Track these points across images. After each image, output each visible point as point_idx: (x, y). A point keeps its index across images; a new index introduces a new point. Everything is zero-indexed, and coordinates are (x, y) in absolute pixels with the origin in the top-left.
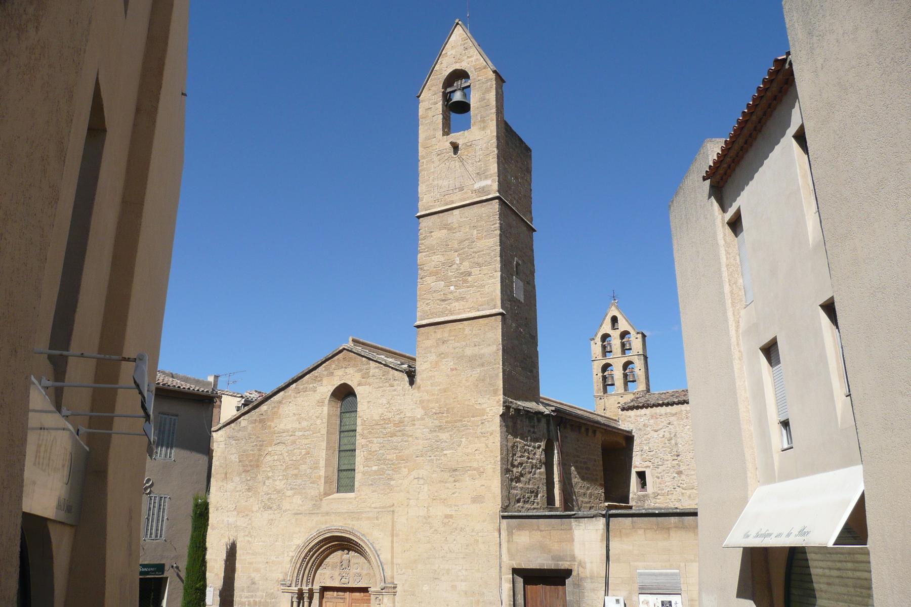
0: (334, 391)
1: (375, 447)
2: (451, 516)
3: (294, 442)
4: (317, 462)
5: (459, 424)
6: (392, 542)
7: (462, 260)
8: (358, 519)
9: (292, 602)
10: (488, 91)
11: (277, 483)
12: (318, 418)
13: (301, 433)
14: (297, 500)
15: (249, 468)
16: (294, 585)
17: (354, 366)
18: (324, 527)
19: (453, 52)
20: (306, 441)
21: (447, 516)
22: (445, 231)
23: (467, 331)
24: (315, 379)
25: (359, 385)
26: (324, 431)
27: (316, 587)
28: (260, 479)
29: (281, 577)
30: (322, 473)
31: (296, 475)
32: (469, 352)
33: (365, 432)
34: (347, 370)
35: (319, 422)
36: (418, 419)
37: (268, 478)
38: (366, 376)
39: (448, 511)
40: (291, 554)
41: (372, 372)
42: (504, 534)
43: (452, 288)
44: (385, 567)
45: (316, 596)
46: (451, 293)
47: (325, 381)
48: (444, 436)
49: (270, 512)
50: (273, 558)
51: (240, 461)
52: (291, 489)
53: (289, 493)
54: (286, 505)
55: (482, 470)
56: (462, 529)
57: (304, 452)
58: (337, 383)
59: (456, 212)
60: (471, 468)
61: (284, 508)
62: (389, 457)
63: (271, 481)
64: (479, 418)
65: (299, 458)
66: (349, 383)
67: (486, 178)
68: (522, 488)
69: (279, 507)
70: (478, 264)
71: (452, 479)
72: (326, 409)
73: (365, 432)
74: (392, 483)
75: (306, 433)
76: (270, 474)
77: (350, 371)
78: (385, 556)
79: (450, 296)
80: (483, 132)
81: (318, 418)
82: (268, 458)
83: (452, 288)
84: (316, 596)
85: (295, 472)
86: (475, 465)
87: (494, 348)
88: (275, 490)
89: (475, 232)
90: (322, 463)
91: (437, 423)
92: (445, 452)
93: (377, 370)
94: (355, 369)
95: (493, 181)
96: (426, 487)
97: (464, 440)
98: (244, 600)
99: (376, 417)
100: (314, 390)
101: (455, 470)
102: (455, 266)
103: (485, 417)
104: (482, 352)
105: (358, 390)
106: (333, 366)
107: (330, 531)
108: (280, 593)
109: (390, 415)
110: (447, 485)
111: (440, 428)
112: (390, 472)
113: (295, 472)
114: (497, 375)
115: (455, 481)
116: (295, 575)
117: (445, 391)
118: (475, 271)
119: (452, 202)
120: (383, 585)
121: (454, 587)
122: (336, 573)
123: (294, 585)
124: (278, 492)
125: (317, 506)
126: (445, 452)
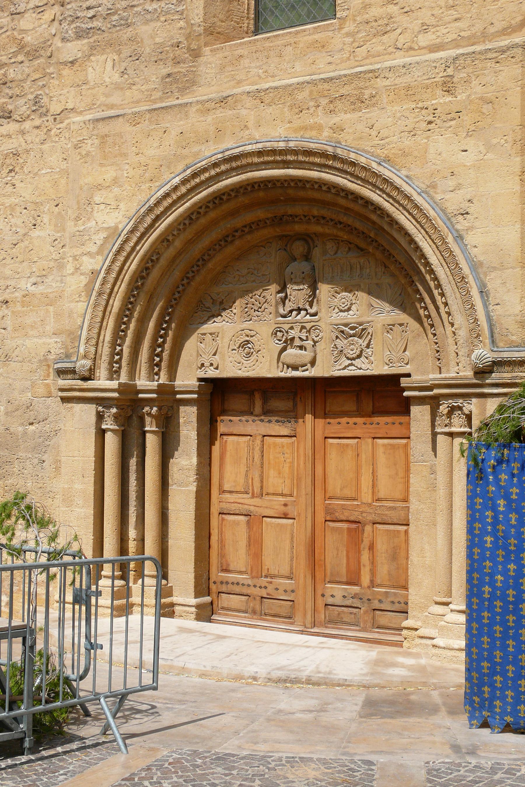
8: (359, 102)
9: (101, 433)
11: (27, 22)
14: (103, 70)
16: (102, 372)
18: (210, 152)
27: (187, 379)
29: (54, 346)
40: (90, 264)
44: (493, 282)
45: (188, 419)
50: (26, 285)
52: (80, 35)
53: (73, 49)
54: (61, 95)
61: (55, 108)
69: (38, 106)
78: (487, 236)
84: (188, 419)
107: (234, 162)
108: (54, 403)
116: (108, 335)
120: (484, 353)
123: (102, 372)
124: (33, 54)
125: (179, 82)
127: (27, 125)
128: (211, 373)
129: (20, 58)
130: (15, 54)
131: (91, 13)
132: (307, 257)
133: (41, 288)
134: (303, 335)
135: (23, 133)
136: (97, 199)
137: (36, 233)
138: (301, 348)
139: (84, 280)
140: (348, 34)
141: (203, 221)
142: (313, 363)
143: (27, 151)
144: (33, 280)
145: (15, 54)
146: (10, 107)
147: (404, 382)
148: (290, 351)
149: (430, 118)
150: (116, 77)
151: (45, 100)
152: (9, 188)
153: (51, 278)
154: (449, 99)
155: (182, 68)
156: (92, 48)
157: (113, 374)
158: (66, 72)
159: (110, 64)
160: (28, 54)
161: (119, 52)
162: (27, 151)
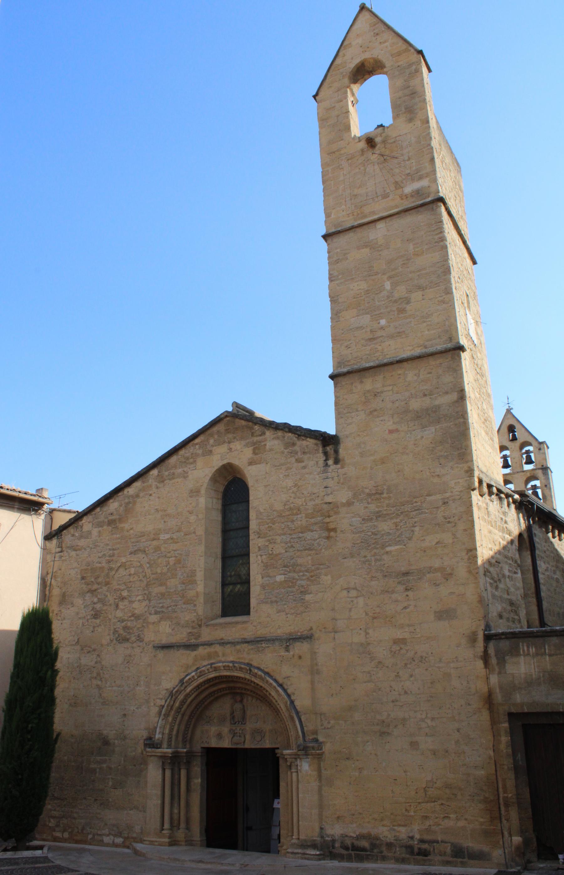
0: (214, 475)
1: (279, 549)
2: (403, 641)
3: (157, 548)
4: (193, 573)
5: (407, 508)
6: (312, 682)
7: (394, 285)
12: (191, 513)
13: (167, 536)
15: (95, 587)
16: (165, 745)
17: (242, 438)
19: (360, 41)
20: (175, 546)
21: (396, 642)
22: (366, 251)
24: (186, 462)
25: (250, 463)
26: (201, 531)
27: (197, 748)
28: (112, 601)
30: (200, 588)
31: (163, 595)
32: (415, 405)
33: (262, 528)
34: (232, 446)
35: (193, 518)
36: (344, 505)
37: (123, 599)
38: (257, 449)
39: (399, 634)
41: (269, 444)
43: (383, 322)
46: (382, 328)
47: (200, 462)
48: (385, 526)
49: (127, 645)
51: (83, 578)
52: (156, 613)
53: (153, 618)
55: (449, 570)
56: (422, 659)
57: (172, 560)
59: (381, 225)
60: (431, 570)
62: (300, 561)
63: (126, 602)
64: (439, 497)
65: (165, 570)
66: (236, 462)
67: (421, 178)
71: (401, 588)
72: (202, 501)
73: (262, 528)
74: (308, 597)
76: (125, 594)
77: (237, 445)
80: (411, 125)
81: (191, 513)
82: (122, 572)
85: (162, 589)
86: (437, 564)
88: (133, 615)
89: (411, 246)
90: (200, 576)
91: (373, 507)
92: (388, 549)
93: (276, 442)
94: (243, 443)
96: (361, 601)
97: (417, 529)
98: (93, 766)
99: (279, 507)
100: (185, 476)
101: (406, 574)
102: (385, 293)
103: (448, 495)
104: (437, 403)
106: (212, 441)
109: (299, 502)
110: (394, 596)
111: (379, 515)
112: (303, 583)
113: (162, 589)
115: (407, 590)
117: (383, 461)
118: (416, 296)
121: (414, 745)
122: (225, 730)
123: (165, 745)
126: (388, 549)
127: (135, 645)
128: (206, 745)
129: (132, 618)
130: (130, 617)
131: (161, 605)
132: (241, 701)
133: (140, 710)
134: (241, 732)
135: (133, 648)
136: (163, 677)
137: (138, 688)
138: (240, 736)
139: (157, 709)
140: (254, 626)
141: (203, 688)
142: (244, 742)
143: (135, 655)
144: (136, 706)
145: (130, 617)
146: (128, 637)
147: (277, 751)
148: (235, 738)
149: (281, 659)
150: (170, 631)
151: (142, 636)
152: (127, 669)
153: (144, 706)
154: (287, 653)
155: (195, 631)
156: (161, 619)
157: (169, 746)
158: (151, 626)
159: (168, 624)
160: (136, 617)
161: (172, 622)
162: (135, 655)
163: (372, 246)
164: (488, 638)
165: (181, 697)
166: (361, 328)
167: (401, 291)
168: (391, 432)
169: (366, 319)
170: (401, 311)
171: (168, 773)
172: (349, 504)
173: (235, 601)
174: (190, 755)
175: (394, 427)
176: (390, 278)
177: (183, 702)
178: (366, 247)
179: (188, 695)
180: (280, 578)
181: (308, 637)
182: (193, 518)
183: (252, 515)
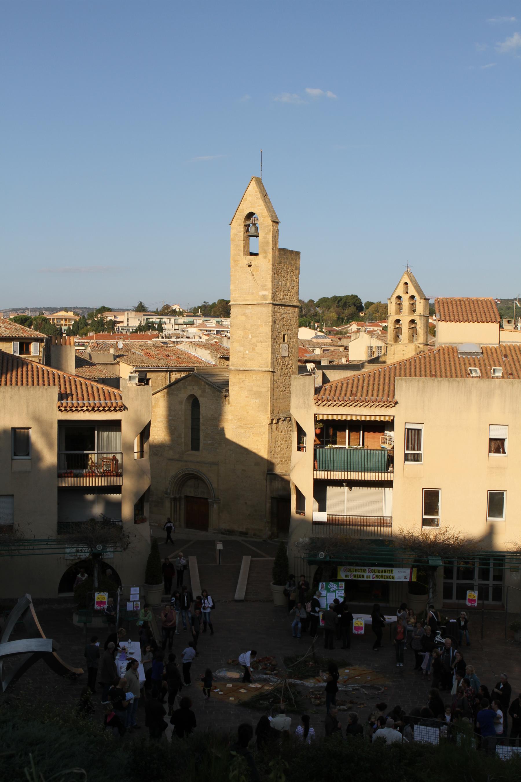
7: (252, 337)
10: (267, 233)
23: (254, 377)
25: (201, 396)
30: (183, 440)
32: (254, 389)
42: (268, 481)
46: (247, 354)
48: (242, 431)
58: (189, 393)
59: (250, 307)
64: (258, 424)
67: (266, 290)
68: (280, 458)
70: (260, 341)
72: (183, 407)
74: (218, 450)
75: (174, 418)
77: (196, 388)
79: (246, 356)
83: (247, 352)
87: (266, 389)
95: (269, 292)
102: (248, 339)
104: (261, 390)
105: (201, 400)
111: (241, 426)
114: (268, 404)
118: (259, 344)
119: (247, 300)
163: (245, 315)
164: (268, 474)
165: (177, 479)
166: (240, 352)
167: (254, 340)
168: (246, 397)
169: (241, 348)
170: (254, 349)
171: (173, 504)
172: (232, 420)
173: (195, 445)
174: (180, 498)
175: (247, 395)
176: (251, 333)
177: (177, 480)
178: (244, 315)
179: (179, 478)
180: (209, 442)
181: (216, 464)
182: (180, 413)
183: (201, 417)
